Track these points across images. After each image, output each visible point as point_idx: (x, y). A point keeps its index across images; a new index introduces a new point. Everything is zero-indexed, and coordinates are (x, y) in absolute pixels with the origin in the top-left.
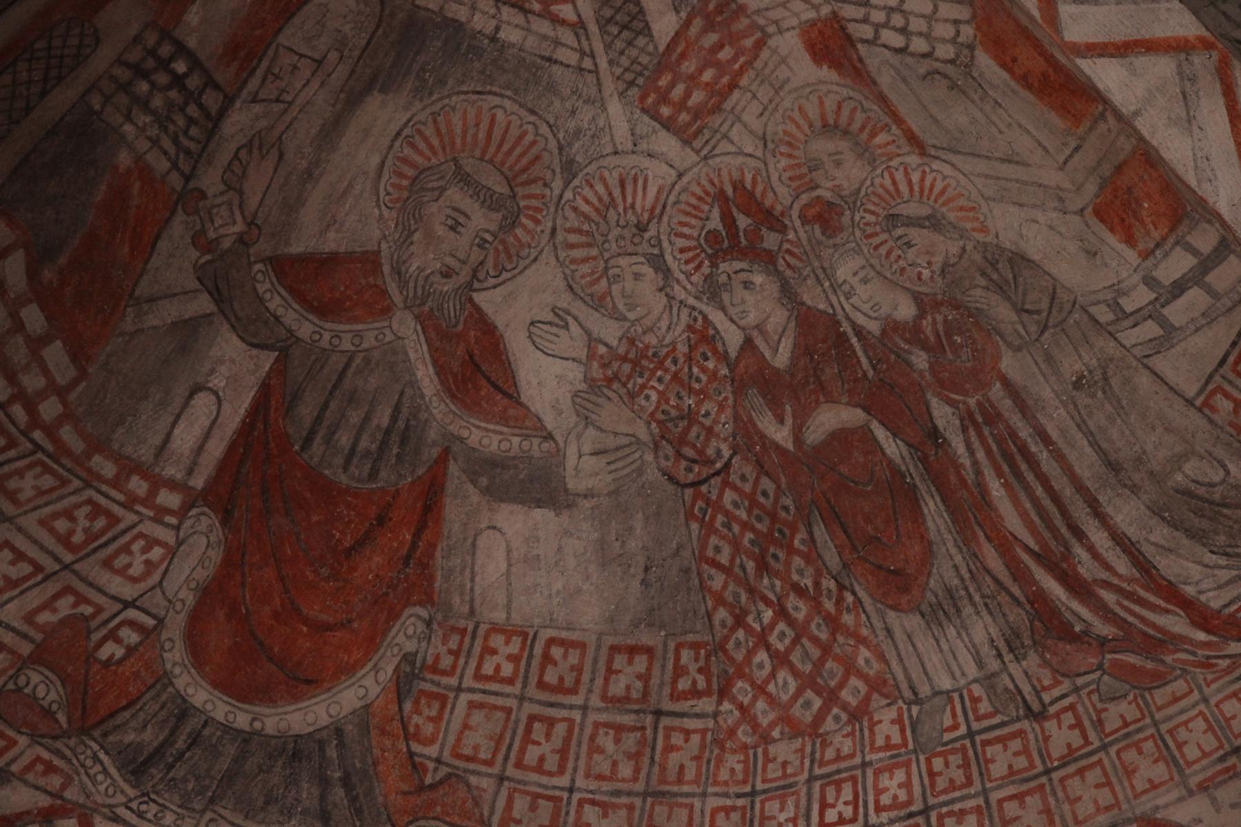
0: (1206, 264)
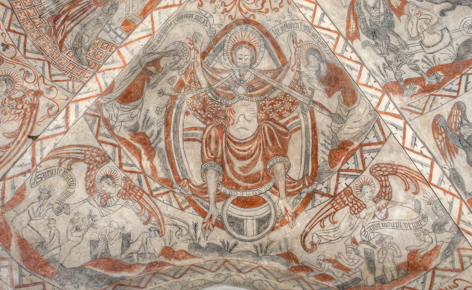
0: (119, 36)
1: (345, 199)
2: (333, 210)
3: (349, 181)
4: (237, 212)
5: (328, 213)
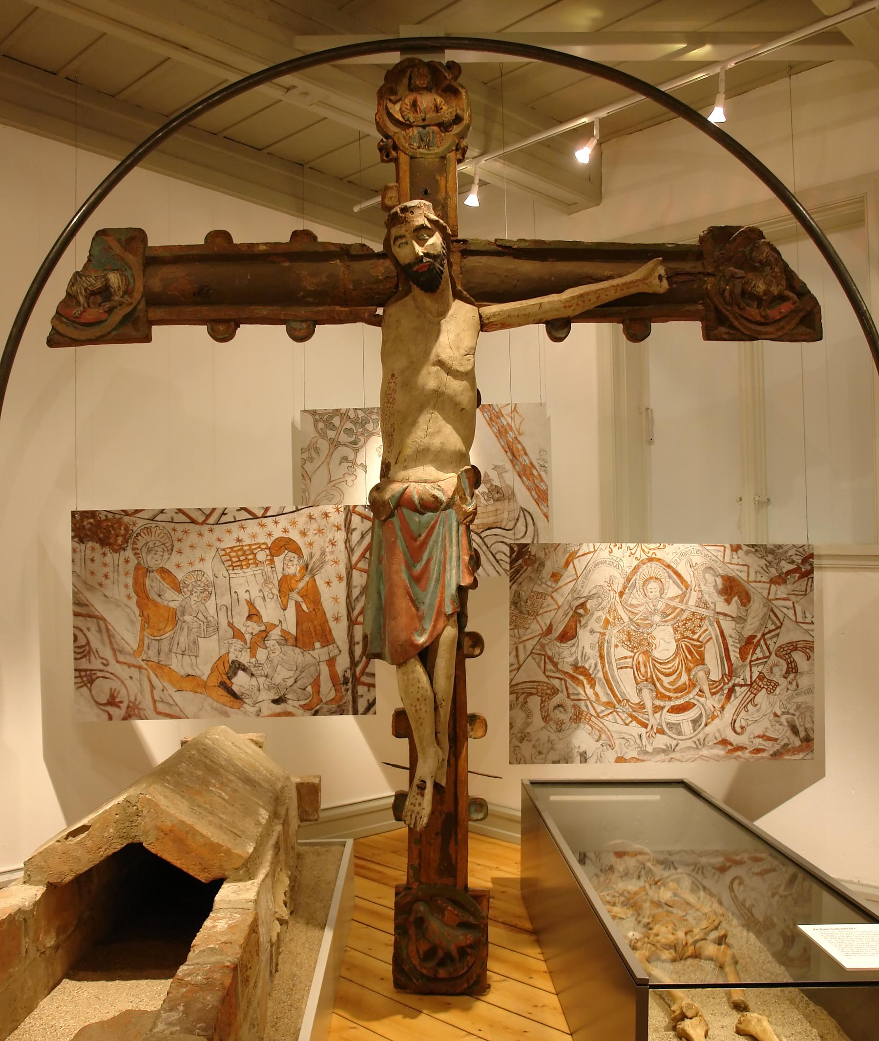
1: (760, 683)
2: (753, 695)
3: (760, 668)
4: (674, 718)
5: (749, 699)
